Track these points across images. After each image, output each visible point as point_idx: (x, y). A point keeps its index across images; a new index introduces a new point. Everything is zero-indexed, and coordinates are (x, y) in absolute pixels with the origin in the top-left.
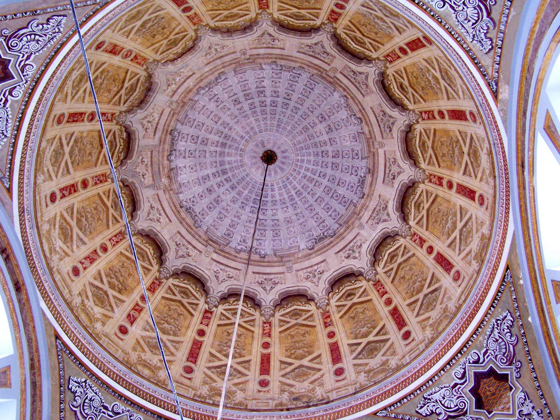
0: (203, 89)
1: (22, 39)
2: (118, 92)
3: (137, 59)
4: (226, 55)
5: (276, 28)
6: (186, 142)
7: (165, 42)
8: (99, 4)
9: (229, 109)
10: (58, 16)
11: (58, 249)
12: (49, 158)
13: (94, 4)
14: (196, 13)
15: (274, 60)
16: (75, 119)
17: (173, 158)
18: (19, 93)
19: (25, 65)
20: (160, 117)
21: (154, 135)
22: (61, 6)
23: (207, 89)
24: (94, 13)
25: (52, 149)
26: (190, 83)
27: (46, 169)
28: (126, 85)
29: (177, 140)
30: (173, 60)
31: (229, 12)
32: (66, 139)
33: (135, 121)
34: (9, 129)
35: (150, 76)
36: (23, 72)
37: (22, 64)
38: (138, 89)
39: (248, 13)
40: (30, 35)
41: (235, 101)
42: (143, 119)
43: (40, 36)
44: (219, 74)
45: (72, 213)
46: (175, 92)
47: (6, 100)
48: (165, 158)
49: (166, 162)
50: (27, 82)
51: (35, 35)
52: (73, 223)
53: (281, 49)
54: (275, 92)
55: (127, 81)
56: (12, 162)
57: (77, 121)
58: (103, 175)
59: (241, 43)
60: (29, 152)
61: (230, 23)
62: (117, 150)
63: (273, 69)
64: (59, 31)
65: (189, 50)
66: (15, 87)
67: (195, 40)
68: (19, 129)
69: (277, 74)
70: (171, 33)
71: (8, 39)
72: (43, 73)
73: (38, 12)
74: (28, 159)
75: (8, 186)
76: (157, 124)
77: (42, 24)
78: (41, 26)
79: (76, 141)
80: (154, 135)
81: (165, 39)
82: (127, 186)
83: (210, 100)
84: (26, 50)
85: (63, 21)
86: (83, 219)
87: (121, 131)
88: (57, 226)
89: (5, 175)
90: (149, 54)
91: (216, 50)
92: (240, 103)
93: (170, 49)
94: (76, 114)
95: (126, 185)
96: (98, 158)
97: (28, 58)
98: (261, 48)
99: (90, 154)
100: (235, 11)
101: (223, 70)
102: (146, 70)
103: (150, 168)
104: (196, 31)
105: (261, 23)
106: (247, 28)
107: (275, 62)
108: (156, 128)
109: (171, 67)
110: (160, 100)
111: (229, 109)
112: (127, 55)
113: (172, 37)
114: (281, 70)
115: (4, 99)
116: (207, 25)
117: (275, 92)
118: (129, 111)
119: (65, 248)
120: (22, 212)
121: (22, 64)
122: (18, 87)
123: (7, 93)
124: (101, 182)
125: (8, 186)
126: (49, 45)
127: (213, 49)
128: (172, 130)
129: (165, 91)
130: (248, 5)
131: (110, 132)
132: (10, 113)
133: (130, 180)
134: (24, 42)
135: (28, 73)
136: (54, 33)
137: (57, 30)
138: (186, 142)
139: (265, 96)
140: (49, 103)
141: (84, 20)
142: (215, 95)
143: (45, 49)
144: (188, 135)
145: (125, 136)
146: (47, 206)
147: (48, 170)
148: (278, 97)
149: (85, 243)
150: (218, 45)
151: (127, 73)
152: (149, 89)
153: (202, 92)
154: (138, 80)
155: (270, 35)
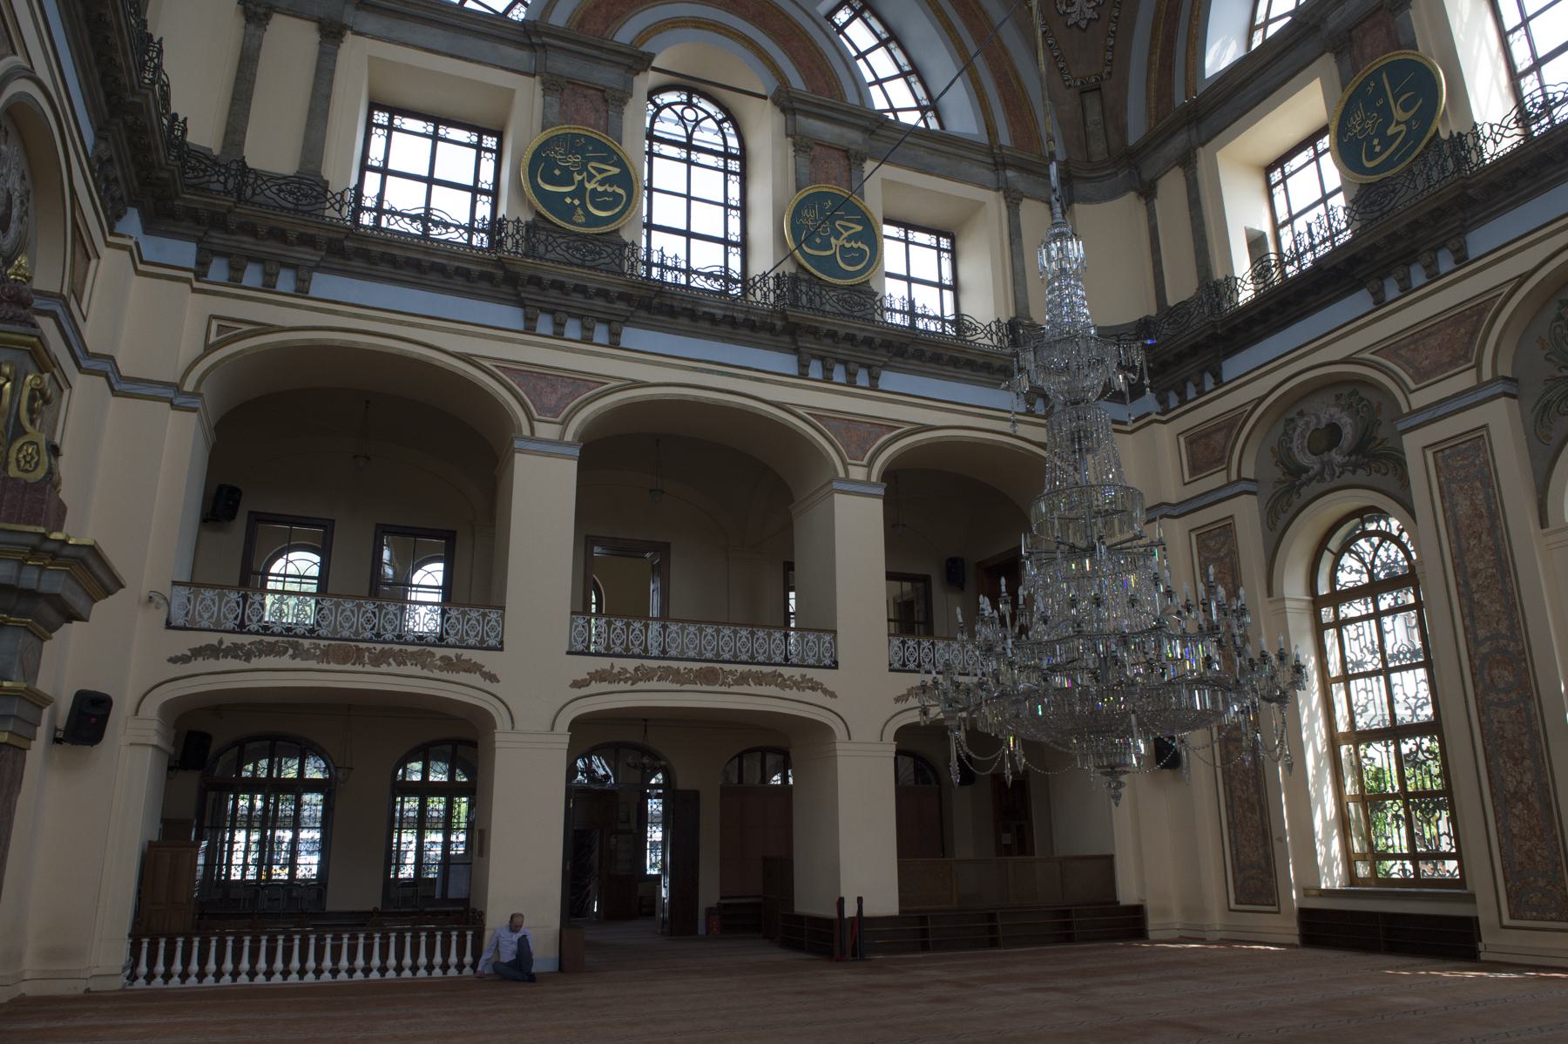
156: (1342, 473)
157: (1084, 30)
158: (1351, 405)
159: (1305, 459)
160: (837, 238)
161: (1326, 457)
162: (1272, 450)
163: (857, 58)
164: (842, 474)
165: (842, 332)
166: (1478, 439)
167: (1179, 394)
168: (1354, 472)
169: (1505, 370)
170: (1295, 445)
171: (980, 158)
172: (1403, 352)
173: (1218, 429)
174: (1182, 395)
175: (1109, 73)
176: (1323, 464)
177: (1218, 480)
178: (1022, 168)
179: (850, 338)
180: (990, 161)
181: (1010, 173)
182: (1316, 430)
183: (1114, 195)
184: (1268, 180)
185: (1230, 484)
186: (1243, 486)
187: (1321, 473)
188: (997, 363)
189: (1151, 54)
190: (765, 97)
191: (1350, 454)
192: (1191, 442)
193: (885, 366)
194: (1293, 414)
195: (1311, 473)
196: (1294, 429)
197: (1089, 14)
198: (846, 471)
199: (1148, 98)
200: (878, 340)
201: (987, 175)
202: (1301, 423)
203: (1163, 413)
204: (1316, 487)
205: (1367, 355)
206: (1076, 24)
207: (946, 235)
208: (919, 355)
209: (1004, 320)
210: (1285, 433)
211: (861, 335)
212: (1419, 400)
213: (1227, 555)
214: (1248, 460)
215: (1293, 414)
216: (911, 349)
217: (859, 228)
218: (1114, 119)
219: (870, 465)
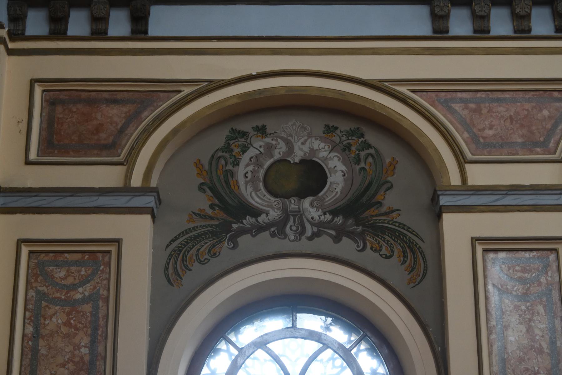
156: (315, 235)
158: (349, 146)
159: (257, 197)
161: (293, 204)
162: (198, 164)
166: (102, 256)
168: (337, 239)
169: (154, 183)
170: (241, 171)
172: (457, 107)
185: (126, 189)
191: (334, 213)
192: (51, 102)
195: (262, 219)
196: (244, 149)
202: (258, 143)
204: (266, 242)
205: (404, 90)
210: (227, 148)
212: (479, 175)
213: (85, 300)
215: (246, 126)
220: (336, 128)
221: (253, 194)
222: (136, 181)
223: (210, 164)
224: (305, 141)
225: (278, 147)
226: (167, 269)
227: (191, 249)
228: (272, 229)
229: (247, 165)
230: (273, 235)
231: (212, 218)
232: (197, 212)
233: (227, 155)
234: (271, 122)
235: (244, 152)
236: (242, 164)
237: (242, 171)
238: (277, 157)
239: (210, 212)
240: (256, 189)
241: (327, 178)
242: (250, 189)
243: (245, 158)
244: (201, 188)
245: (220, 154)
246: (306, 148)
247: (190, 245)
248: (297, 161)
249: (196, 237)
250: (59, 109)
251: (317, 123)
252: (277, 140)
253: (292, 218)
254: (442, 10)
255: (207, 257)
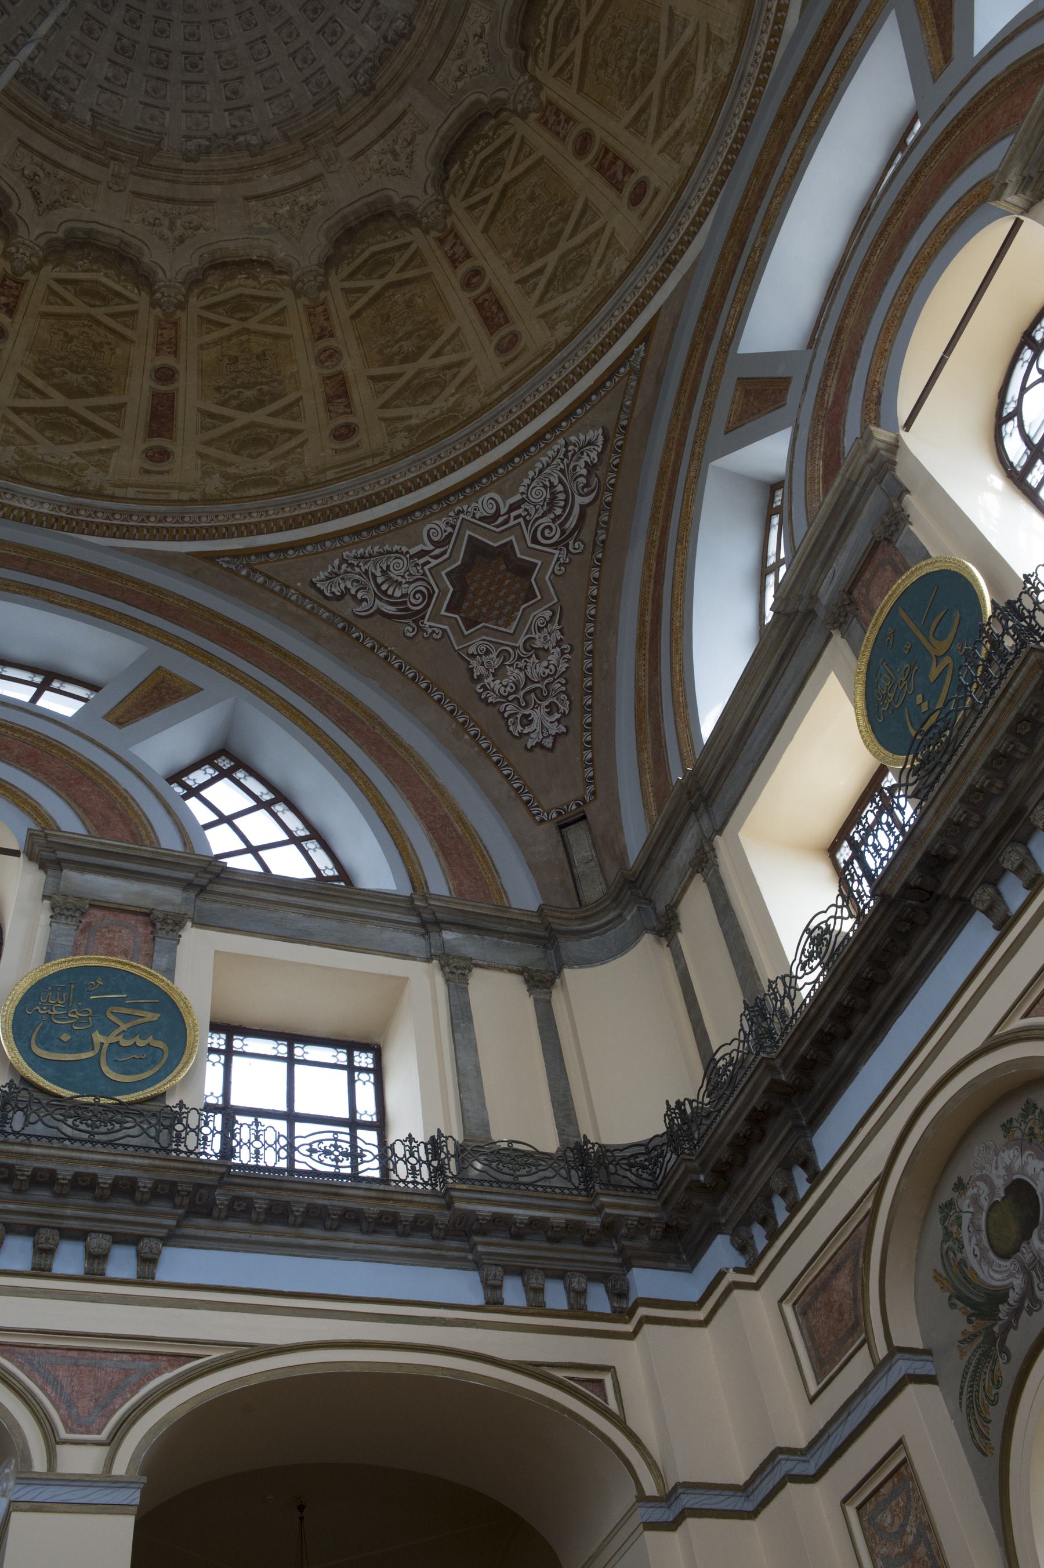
0: (248, 146)
1: (403, 596)
2: (400, 284)
3: (323, 329)
4: (158, 198)
5: (13, 210)
6: (351, 40)
7: (253, 324)
8: (248, 565)
9: (219, 53)
10: (321, 592)
11: (709, 77)
12: (580, 288)
13: (255, 571)
14: (158, 351)
15: (57, 124)
16: (494, 308)
17: (400, 24)
18: (485, 504)
19: (437, 544)
20: (369, 146)
21: (404, 113)
22: (304, 608)
23: (241, 138)
24: (267, 553)
25: (562, 299)
26: (266, 181)
27: (600, 271)
28: (377, 285)
29: (367, 60)
30: (266, 264)
31: (93, 311)
32: (536, 284)
33: (412, 188)
34: (550, 453)
35: (329, 263)
36: (451, 534)
37: (438, 551)
38: (366, 254)
39: (55, 286)
40: (385, 593)
41: (194, 66)
42: (401, 173)
43: (374, 577)
44: (195, 160)
45: (642, 110)
46: (307, 184)
47: (513, 507)
48: (415, 36)
49: (420, 26)
50: (459, 512)
51: (378, 586)
52: (654, 86)
53: (27, 146)
54: (90, 32)
55: (371, 293)
56: (598, 386)
57: (497, 302)
58: (546, 123)
59: (109, 213)
60: (570, 366)
61: (105, 278)
62: (489, 150)
63: (70, 101)
64: (343, 561)
65: (224, 265)
66: (481, 519)
67: (197, 282)
68: (538, 438)
69: (66, 81)
70: (229, 338)
71: (417, 616)
72: (423, 506)
73: (341, 625)
74: (582, 355)
75: (642, 347)
76: (383, 135)
77: (354, 597)
78: (359, 595)
79: (529, 259)
80: (404, 113)
81: (247, 331)
82: (524, 47)
83: (247, 107)
84: (413, 570)
85: (322, 575)
86: (637, 70)
87: (453, 187)
88: (677, 124)
89: (629, 373)
90: (297, 325)
91: (172, 224)
92: (187, 54)
93: (254, 298)
94: (485, 319)
95: (524, 46)
96: (529, 171)
97: (423, 553)
98: (72, 171)
99: (532, 198)
100: (79, 307)
101: (184, 165)
102: (324, 286)
103: (459, 41)
104: (182, 306)
105: (42, 241)
106: (80, 244)
107: (56, 116)
108: (391, 127)
109: (281, 251)
110: (345, 191)
111: (219, 53)
112: (331, 356)
113: (235, 325)
114: (50, 87)
115: (513, 514)
116: (154, 304)
117: (90, 32)
118: (411, 218)
119: (701, 56)
120: (672, 262)
121: (438, 551)
122: (478, 516)
123: (501, 520)
124: (558, 112)
125: (642, 347)
126: (376, 549)
127: (177, 233)
128: (366, 94)
129: (324, 204)
130: (45, 308)
131: (471, 208)
132: (526, 481)
133: (509, 52)
134: (405, 589)
135: (443, 526)
136: (351, 565)
137: (344, 566)
138: (351, 40)
139: (120, 36)
140: (467, 430)
141: (290, 552)
142: (231, 111)
143: (387, 547)
144: (338, 54)
145: (456, 167)
146: (656, 193)
147: (599, 265)
148: (89, 16)
149: (671, 14)
150: (162, 237)
151: (358, 313)
152: (349, 234)
153: (254, 140)
154: (351, 276)
155: (36, 196)
157: (551, 750)
159: (996, 1274)
160: (105, 1033)
162: (937, 1277)
163: (186, 797)
164: (39, 1465)
165: (65, 1172)
167: (763, 1222)
171: (395, 916)
173: (835, 1266)
174: (767, 1219)
175: (594, 793)
176: (1026, 1270)
177: (859, 1368)
178: (469, 925)
179: (84, 1184)
180: (414, 920)
181: (448, 935)
182: (993, 1206)
183: (622, 948)
184: (835, 863)
185: (880, 1367)
186: (902, 1366)
187: (1029, 1291)
188: (408, 1212)
189: (640, 751)
190: (16, 853)
192: (803, 1312)
193: (171, 1238)
194: (947, 1194)
195: (1013, 1297)
196: (959, 1220)
197: (554, 729)
198: (51, 1458)
199: (646, 805)
200: (145, 1182)
201: (412, 941)
203: (750, 1270)
205: (1017, 1023)
206: (539, 745)
207: (365, 1048)
208: (240, 1209)
209: (420, 1137)
210: (948, 1235)
211: (106, 1176)
214: (903, 1314)
215: (947, 1194)
216: (221, 1198)
217: (150, 1016)
218: (608, 843)
219: (114, 1441)
220: (1011, 1120)
221: (992, 1273)
222: (882, 1351)
223: (944, 1266)
224: (997, 1162)
225: (981, 1192)
226: (973, 1436)
227: (978, 1391)
228: (1026, 1305)
229: (970, 1240)
230: (1030, 1312)
231: (975, 1336)
232: (961, 1338)
233: (950, 1243)
234: (962, 1169)
235: (960, 1226)
236: (966, 1243)
237: (970, 1248)
238: (985, 1204)
239: (970, 1328)
240: (990, 1264)
241: (1034, 1191)
242: (985, 1268)
243: (965, 1234)
244: (952, 1306)
245: (945, 1247)
246: (1002, 1172)
247: (975, 1388)
248: (1003, 1195)
249: (975, 1371)
250: (810, 1314)
251: (993, 1134)
252: (976, 1186)
253: (1033, 1273)
254: (983, 902)
255: (994, 1391)
